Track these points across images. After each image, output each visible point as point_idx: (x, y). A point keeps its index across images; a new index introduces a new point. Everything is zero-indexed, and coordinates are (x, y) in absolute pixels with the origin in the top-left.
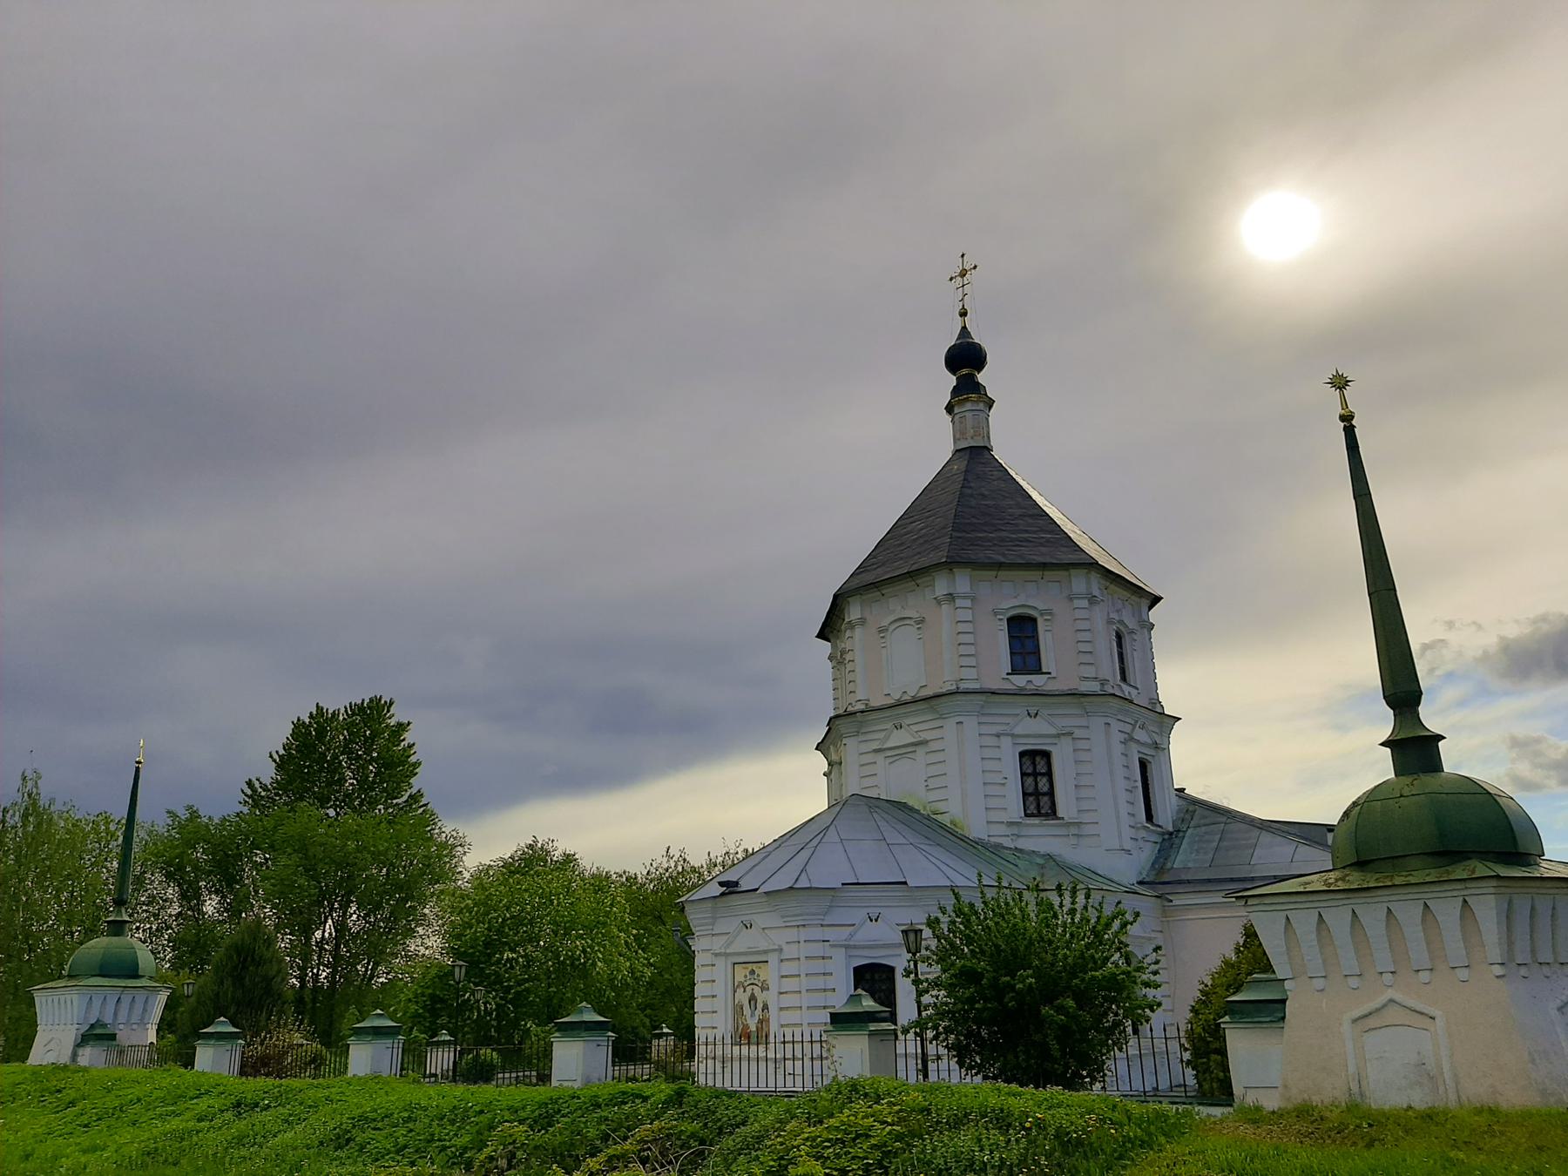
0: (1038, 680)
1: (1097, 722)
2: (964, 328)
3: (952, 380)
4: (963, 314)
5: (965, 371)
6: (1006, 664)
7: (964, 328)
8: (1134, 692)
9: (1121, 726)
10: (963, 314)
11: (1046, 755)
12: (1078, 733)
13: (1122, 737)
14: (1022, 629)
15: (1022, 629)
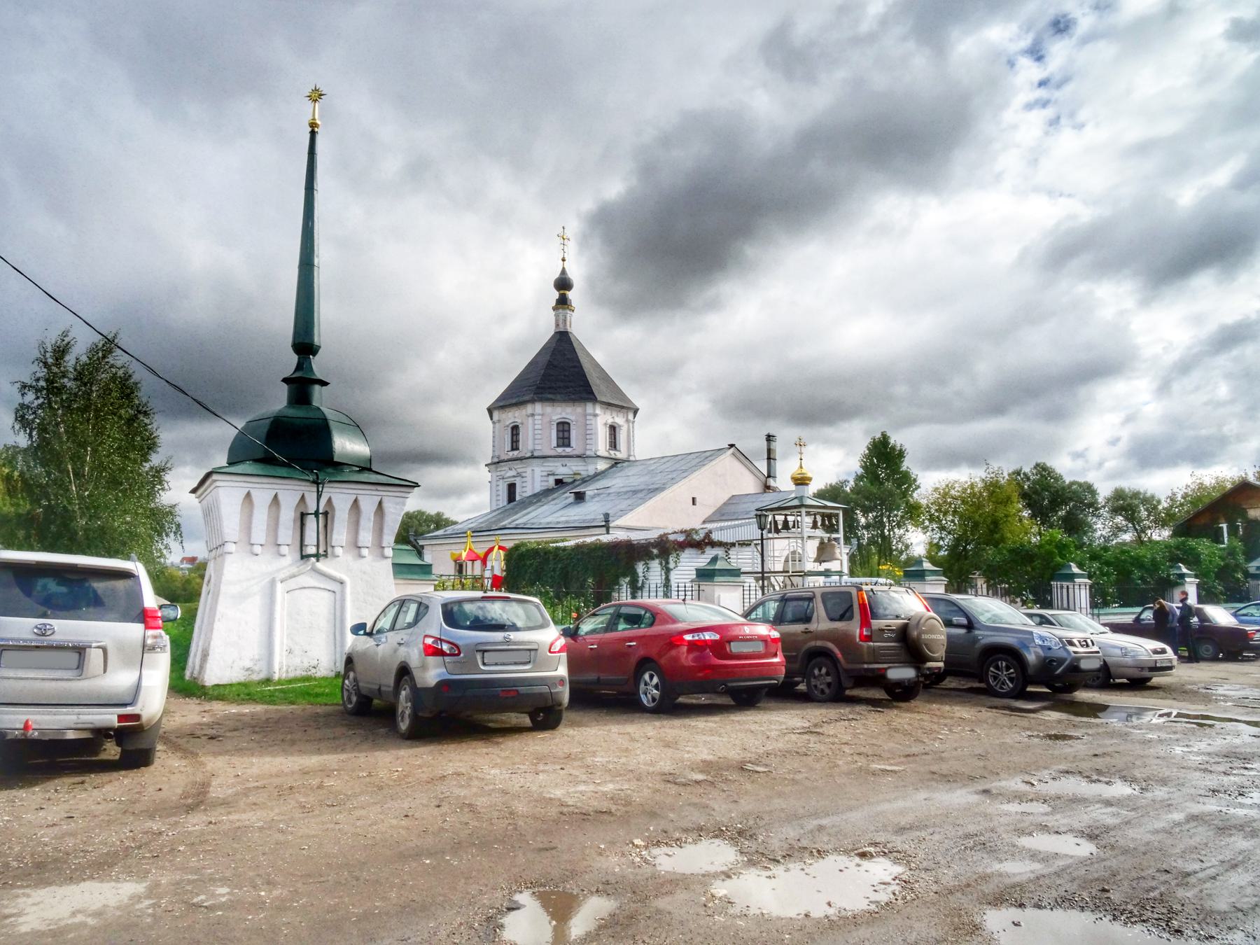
0: (516, 453)
1: (529, 470)
2: (564, 268)
3: (556, 295)
4: (564, 260)
5: (562, 292)
6: (508, 446)
7: (564, 268)
8: (568, 450)
9: (543, 469)
10: (564, 260)
11: (515, 484)
12: (524, 475)
13: (545, 474)
14: (515, 429)
15: (515, 429)
